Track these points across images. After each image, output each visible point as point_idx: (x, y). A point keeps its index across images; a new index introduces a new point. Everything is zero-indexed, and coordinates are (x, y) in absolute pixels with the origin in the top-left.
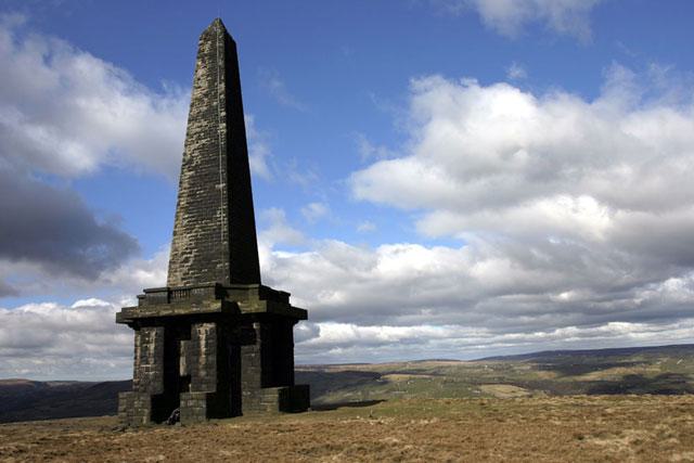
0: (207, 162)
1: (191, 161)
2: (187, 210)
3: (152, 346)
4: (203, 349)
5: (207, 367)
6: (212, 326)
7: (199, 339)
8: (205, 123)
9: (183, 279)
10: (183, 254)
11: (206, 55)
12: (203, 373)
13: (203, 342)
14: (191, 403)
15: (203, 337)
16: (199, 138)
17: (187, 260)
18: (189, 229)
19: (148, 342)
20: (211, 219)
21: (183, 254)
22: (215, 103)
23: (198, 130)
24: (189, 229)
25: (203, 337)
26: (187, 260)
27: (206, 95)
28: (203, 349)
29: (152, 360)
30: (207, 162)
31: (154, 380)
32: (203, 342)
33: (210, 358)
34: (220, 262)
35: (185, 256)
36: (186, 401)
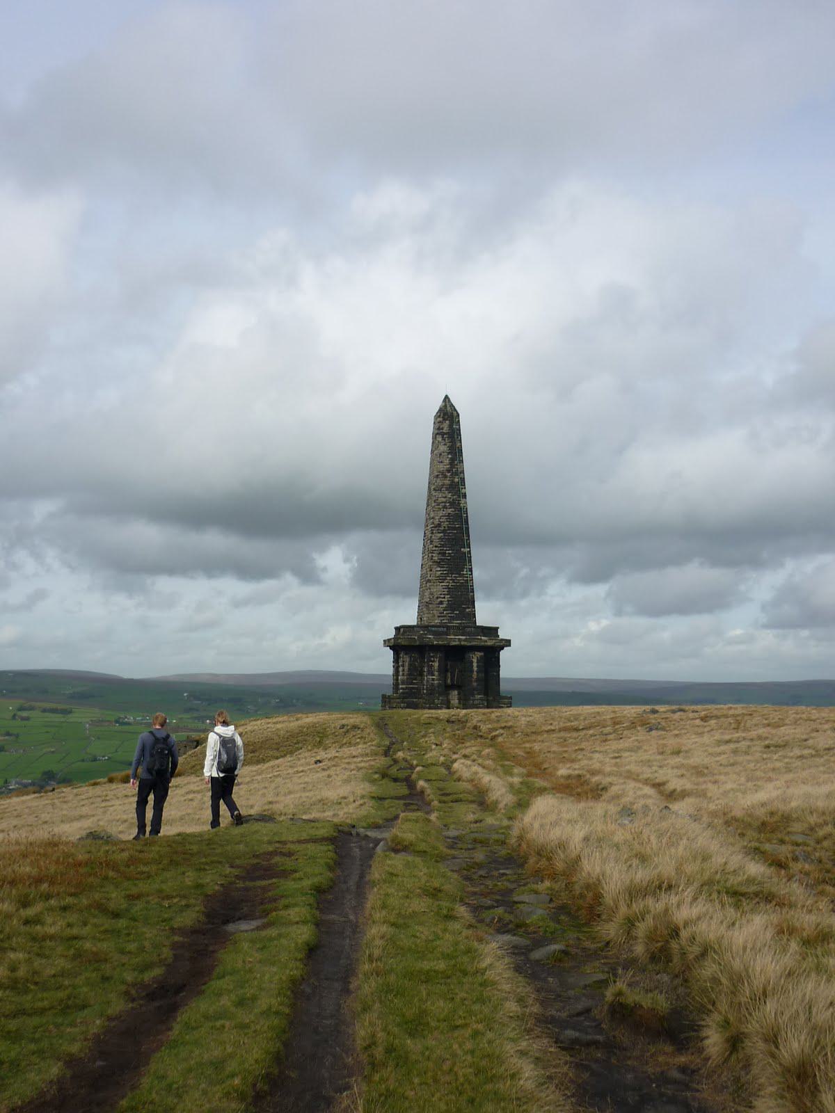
0: (455, 528)
1: (439, 525)
2: (438, 564)
3: (436, 665)
4: (475, 669)
5: (477, 680)
6: (479, 654)
7: (472, 662)
8: (449, 495)
9: (439, 617)
10: (437, 598)
11: (445, 434)
12: (475, 684)
13: (475, 665)
14: (476, 702)
15: (475, 660)
16: (445, 507)
17: (441, 603)
18: (442, 579)
19: (434, 661)
20: (460, 574)
21: (437, 598)
22: (456, 480)
23: (444, 500)
24: (442, 579)
25: (475, 660)
26: (441, 603)
27: (448, 471)
28: (475, 669)
29: (436, 673)
30: (455, 528)
31: (438, 687)
32: (475, 665)
33: (480, 675)
34: (469, 608)
35: (439, 600)
36: (473, 700)
